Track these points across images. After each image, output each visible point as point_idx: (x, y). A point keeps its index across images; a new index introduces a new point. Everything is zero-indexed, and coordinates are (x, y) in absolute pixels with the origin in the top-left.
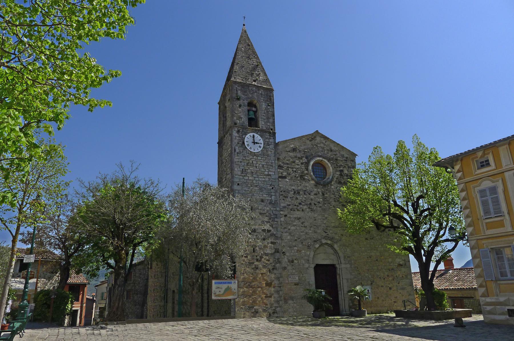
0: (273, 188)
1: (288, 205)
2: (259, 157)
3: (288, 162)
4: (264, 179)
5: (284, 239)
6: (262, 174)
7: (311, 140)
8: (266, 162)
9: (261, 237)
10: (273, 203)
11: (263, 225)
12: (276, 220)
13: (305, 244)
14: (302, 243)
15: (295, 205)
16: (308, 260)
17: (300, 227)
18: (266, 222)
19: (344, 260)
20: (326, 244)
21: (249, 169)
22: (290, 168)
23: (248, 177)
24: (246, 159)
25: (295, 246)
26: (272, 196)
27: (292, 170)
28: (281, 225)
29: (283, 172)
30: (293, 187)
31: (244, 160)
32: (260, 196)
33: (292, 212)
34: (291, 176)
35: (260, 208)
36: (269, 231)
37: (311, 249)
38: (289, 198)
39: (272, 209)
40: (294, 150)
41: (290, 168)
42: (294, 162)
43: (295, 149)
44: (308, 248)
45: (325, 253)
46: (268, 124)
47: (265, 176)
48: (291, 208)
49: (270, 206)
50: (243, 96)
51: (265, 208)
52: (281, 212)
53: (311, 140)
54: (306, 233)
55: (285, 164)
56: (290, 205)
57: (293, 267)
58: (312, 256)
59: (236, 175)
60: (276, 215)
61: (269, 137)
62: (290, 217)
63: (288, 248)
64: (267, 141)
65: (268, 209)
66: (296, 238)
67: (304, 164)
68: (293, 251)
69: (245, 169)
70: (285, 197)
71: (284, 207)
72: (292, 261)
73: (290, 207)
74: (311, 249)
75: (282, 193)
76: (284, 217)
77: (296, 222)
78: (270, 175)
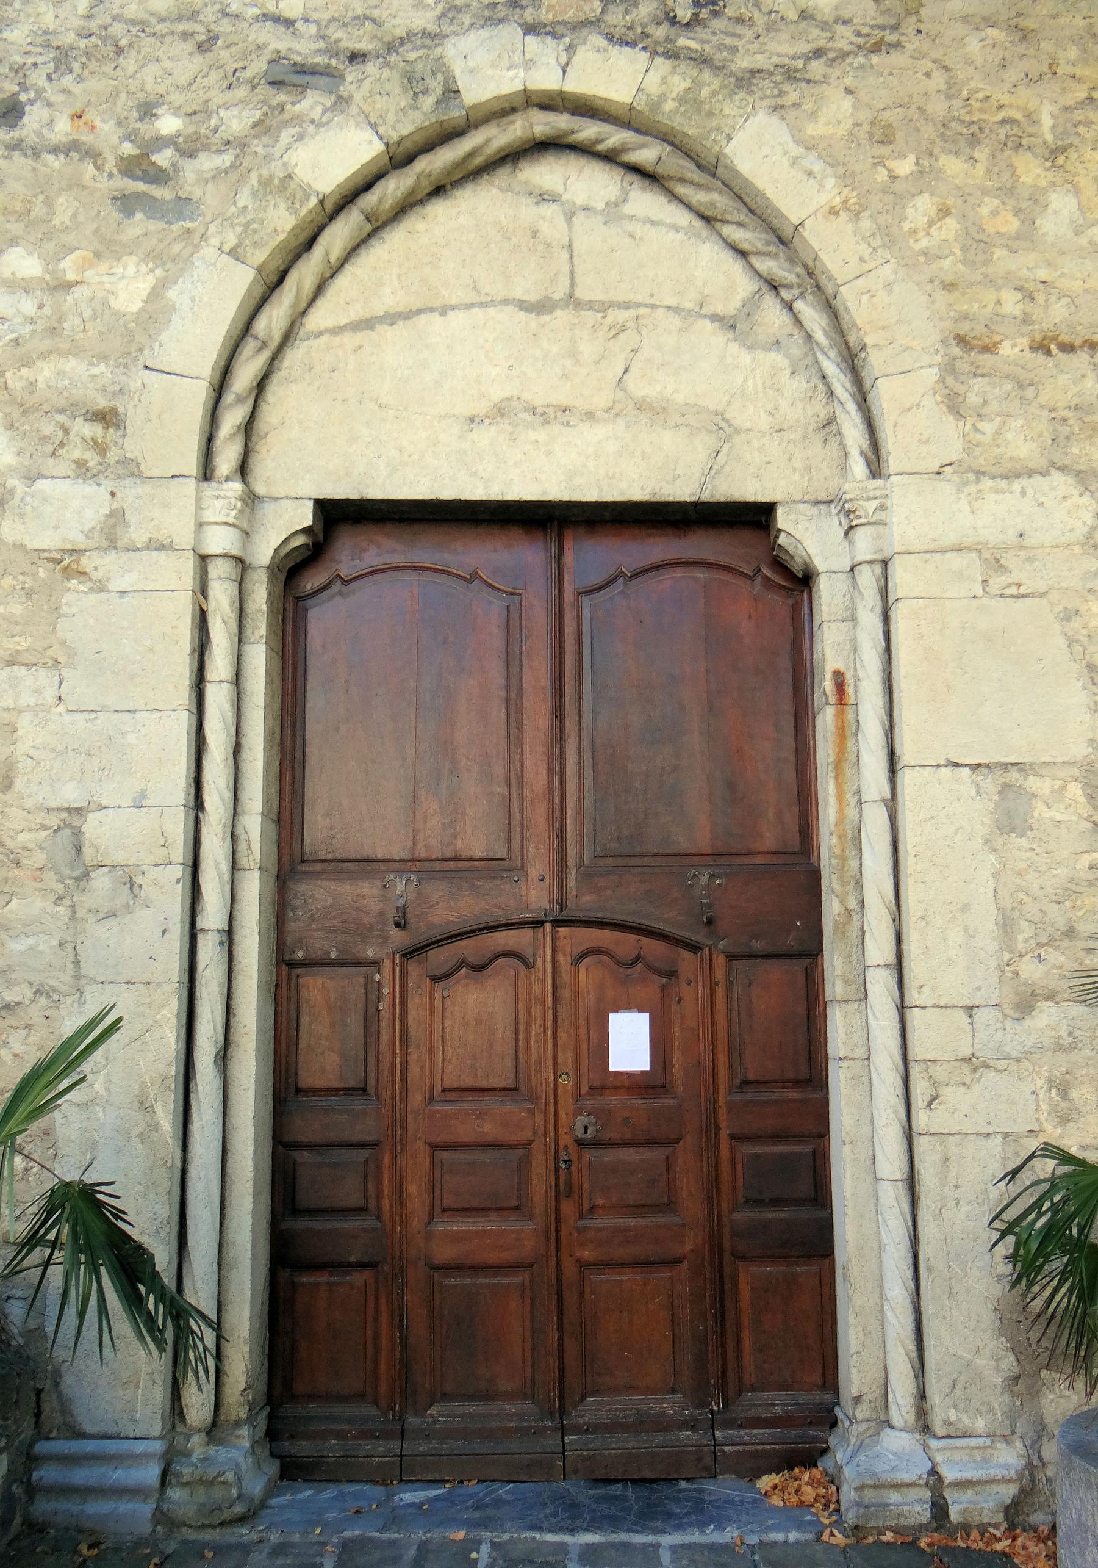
13: (63, 128)
16: (106, 418)
19: (954, 404)
37: (183, 206)
44: (126, 204)
45: (541, 307)
74: (183, 206)
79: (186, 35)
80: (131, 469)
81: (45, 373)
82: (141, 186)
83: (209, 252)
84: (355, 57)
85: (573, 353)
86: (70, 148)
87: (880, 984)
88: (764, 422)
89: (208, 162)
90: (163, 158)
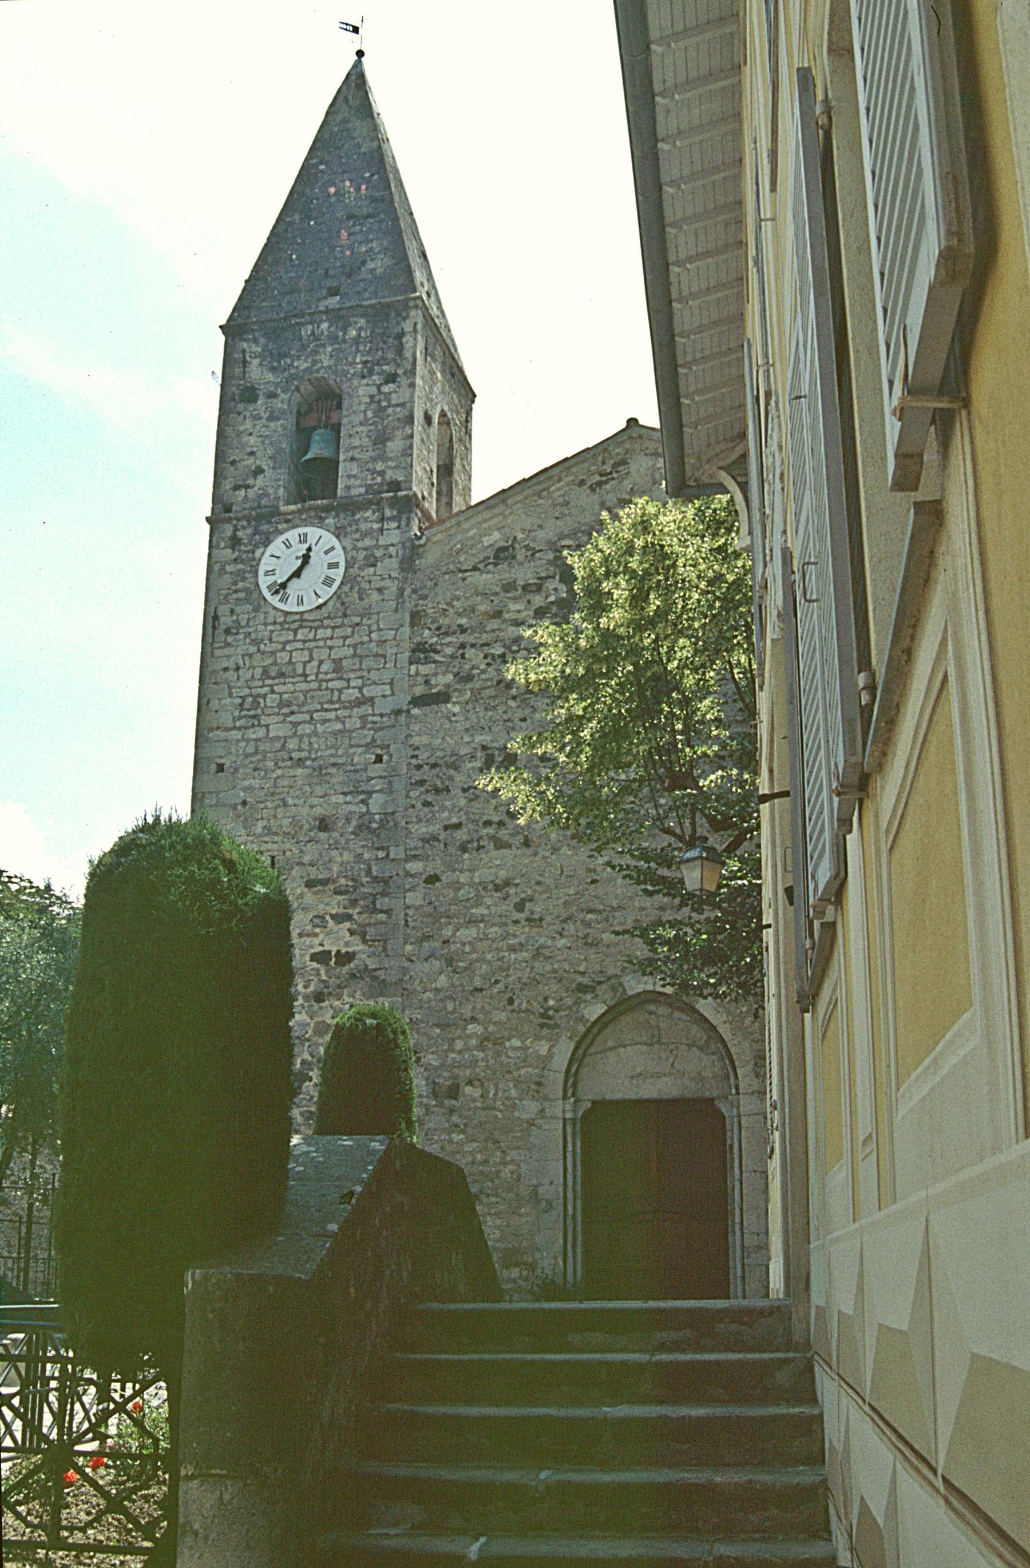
0: (379, 759)
1: (446, 828)
2: (322, 627)
3: (463, 621)
4: (339, 726)
5: (419, 988)
6: (332, 702)
7: (600, 484)
8: (355, 646)
9: (306, 987)
10: (375, 825)
11: (316, 935)
12: (382, 903)
14: (511, 1001)
15: (488, 823)
16: (539, 1084)
17: (506, 925)
18: (332, 916)
20: (654, 997)
21: (273, 692)
22: (473, 646)
23: (267, 726)
24: (263, 653)
25: (474, 1019)
26: (370, 793)
27: (486, 657)
28: (406, 924)
29: (436, 675)
30: (479, 739)
31: (250, 656)
32: (312, 807)
33: (466, 856)
34: (477, 685)
35: (306, 859)
36: (345, 958)
38: (456, 792)
39: (366, 856)
40: (503, 554)
41: (473, 646)
42: (498, 614)
43: (506, 549)
44: (542, 1026)
46: (380, 466)
47: (346, 708)
48: (465, 837)
49: (356, 845)
50: (270, 377)
51: (334, 853)
52: (414, 867)
53: (600, 484)
54: (537, 954)
55: (446, 634)
56: (458, 826)
57: (455, 1119)
58: (561, 1061)
59: (211, 730)
60: (386, 881)
61: (376, 526)
62: (457, 886)
63: (438, 1031)
64: (365, 549)
65: (347, 857)
66: (478, 982)
67: (554, 609)
68: (459, 1045)
69: (256, 697)
70: (437, 791)
71: (430, 840)
72: (454, 1092)
73: (461, 835)
75: (426, 773)
76: (422, 888)
77: (491, 905)
78: (371, 700)
79: (556, 978)
80: (546, 1098)
81: (523, 1071)
82: (545, 1021)
83: (563, 1038)
84: (599, 983)
85: (660, 1058)
86: (527, 1010)
87: (737, 1228)
88: (711, 1075)
89: (562, 1013)
90: (551, 1013)
